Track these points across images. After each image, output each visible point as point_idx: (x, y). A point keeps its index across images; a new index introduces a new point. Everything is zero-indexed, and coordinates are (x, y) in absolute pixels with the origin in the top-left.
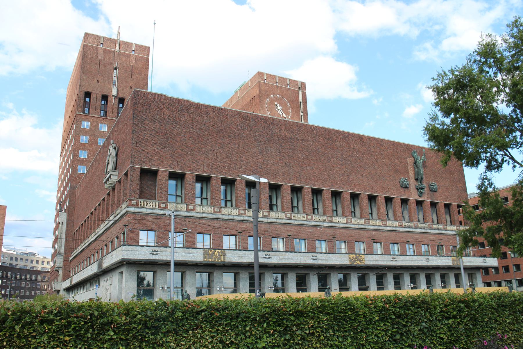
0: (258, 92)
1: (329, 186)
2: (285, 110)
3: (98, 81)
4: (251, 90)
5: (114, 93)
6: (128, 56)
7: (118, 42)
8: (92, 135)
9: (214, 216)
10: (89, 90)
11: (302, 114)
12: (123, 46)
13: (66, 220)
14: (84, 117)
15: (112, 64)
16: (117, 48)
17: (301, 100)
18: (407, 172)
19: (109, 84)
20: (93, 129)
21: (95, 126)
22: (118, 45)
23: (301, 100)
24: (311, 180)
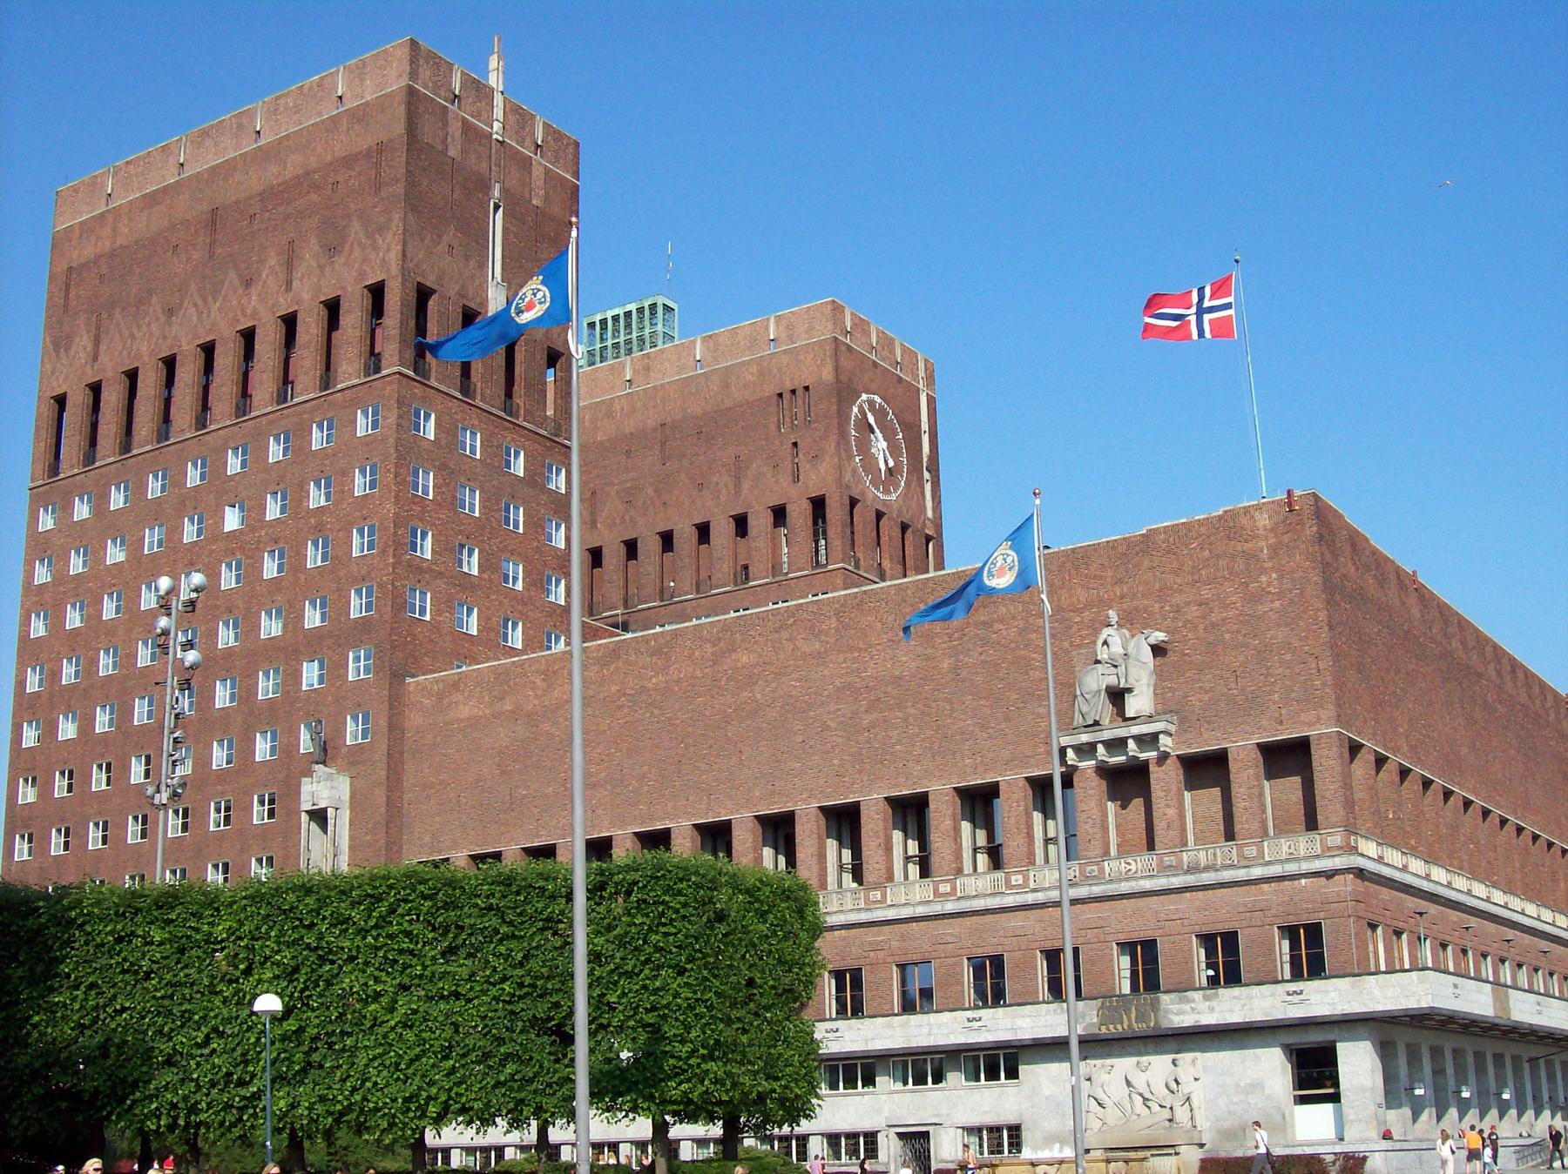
0: (827, 374)
2: (893, 449)
4: (785, 359)
7: (498, 100)
10: (430, 282)
11: (927, 475)
13: (346, 797)
14: (418, 390)
15: (486, 188)
17: (925, 426)
19: (482, 265)
20: (443, 443)
22: (498, 113)
23: (925, 426)
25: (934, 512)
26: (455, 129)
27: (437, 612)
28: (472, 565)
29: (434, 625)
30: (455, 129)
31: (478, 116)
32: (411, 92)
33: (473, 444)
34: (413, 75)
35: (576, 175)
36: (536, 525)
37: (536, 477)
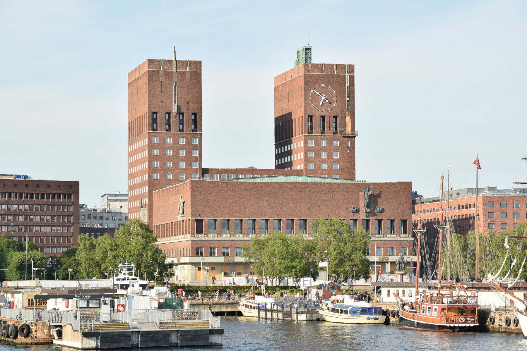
1: (298, 217)
3: (162, 102)
5: (175, 110)
6: (184, 73)
8: (161, 148)
9: (231, 239)
11: (348, 99)
12: (178, 64)
14: (154, 134)
16: (174, 68)
18: (358, 201)
19: (171, 102)
21: (162, 141)
22: (175, 65)
24: (286, 214)
25: (350, 109)
26: (162, 75)
27: (160, 176)
28: (170, 165)
29: (160, 180)
30: (162, 75)
31: (169, 68)
32: (149, 71)
33: (169, 141)
34: (149, 67)
35: (201, 70)
36: (189, 153)
37: (189, 143)
